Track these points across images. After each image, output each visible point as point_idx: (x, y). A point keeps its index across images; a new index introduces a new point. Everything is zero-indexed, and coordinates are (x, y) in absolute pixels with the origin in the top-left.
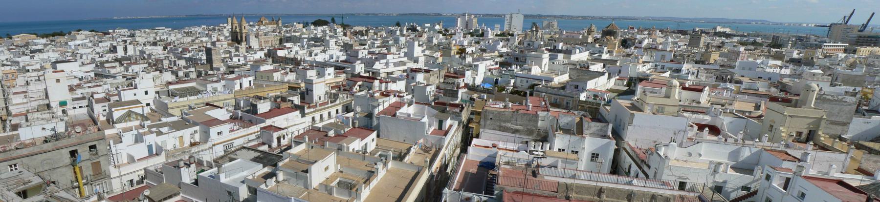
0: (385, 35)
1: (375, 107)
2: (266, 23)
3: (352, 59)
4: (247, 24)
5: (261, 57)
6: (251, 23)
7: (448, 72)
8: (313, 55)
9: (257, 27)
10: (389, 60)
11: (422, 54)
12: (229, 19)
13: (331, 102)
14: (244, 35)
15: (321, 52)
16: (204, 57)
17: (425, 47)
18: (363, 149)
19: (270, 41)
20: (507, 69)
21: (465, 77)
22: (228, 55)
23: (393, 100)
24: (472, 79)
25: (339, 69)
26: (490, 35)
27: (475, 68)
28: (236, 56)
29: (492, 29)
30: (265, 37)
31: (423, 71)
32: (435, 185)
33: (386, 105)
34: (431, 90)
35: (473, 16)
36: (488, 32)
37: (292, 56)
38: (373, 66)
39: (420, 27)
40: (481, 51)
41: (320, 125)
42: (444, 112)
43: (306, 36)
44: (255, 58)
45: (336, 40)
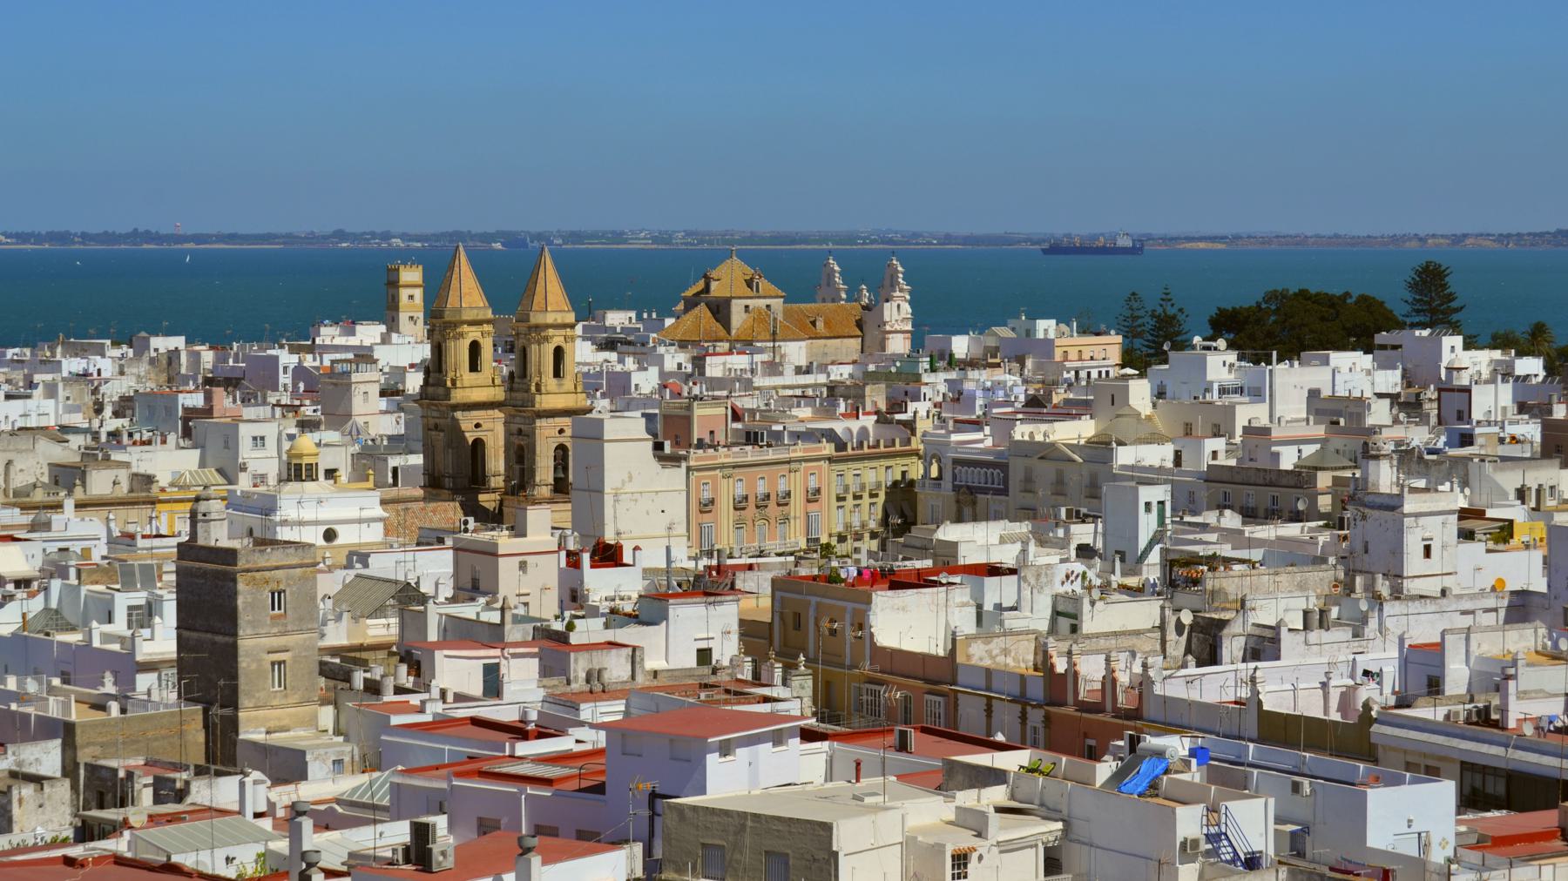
2: (763, 316)
5: (704, 656)
6: (617, 319)
8: (1232, 647)
9: (674, 359)
12: (411, 275)
14: (547, 436)
15: (1315, 620)
16: (162, 641)
22: (383, 629)
28: (463, 634)
30: (751, 454)
37: (1020, 658)
43: (1158, 455)
44: (653, 662)
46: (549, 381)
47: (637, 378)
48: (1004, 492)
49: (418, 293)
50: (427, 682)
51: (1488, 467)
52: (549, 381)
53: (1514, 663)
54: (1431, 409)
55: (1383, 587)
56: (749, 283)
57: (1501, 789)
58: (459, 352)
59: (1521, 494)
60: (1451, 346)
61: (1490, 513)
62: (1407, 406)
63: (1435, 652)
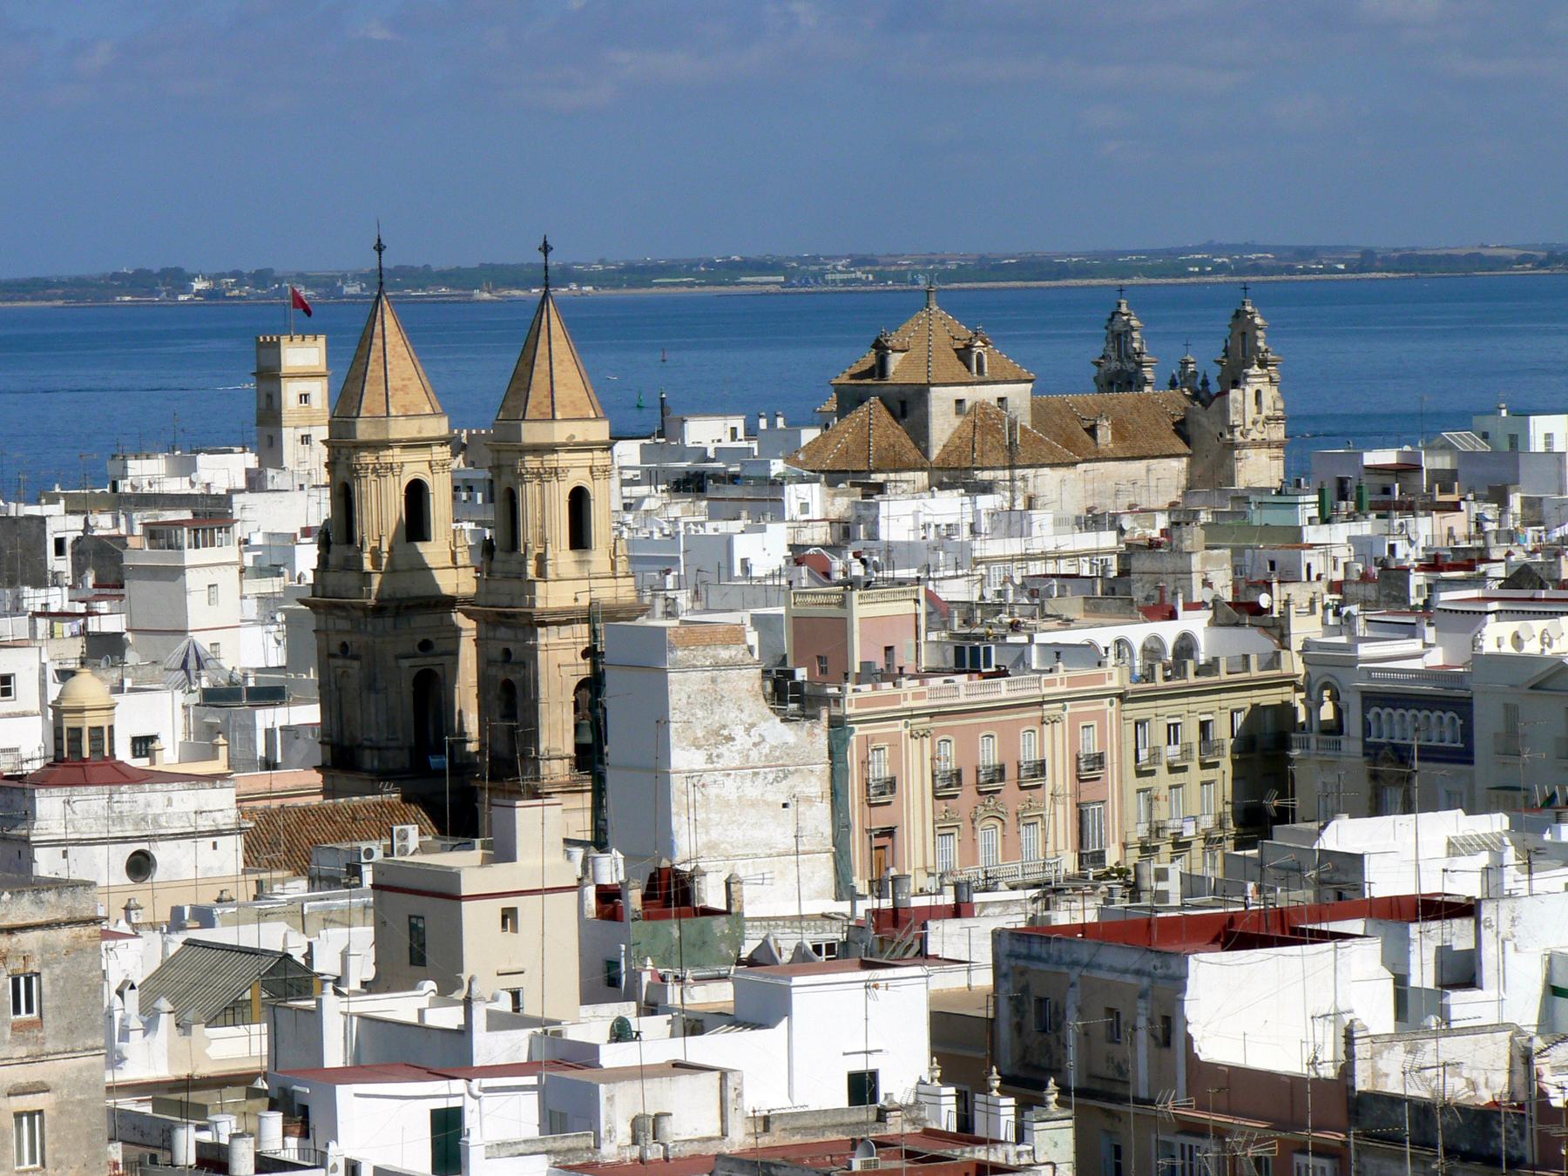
4: (629, 452)
5: (862, 1087)
19: (1059, 776)
46: (562, 557)
47: (744, 546)
48: (1464, 756)
49: (319, 391)
50: (320, 1147)
52: (562, 557)
56: (964, 354)
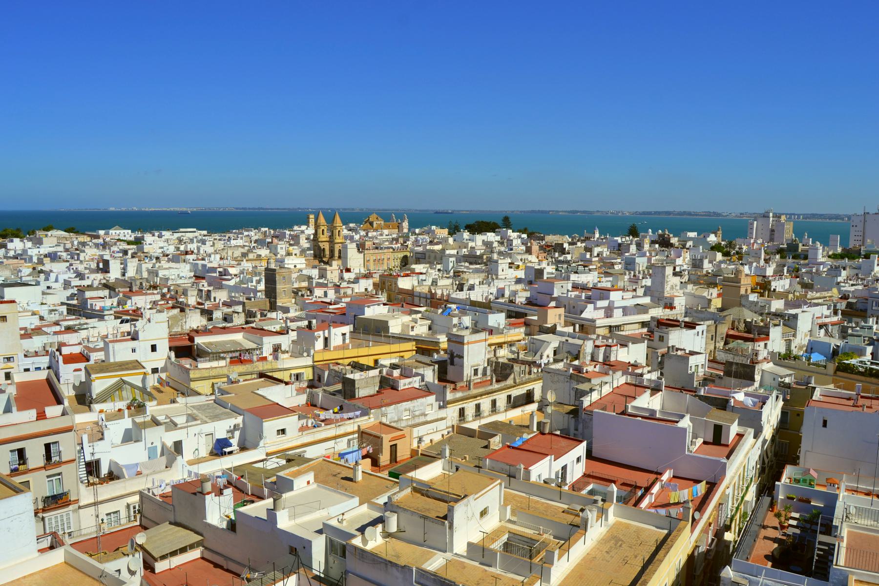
0: (606, 252)
1: (584, 393)
2: (379, 225)
3: (541, 299)
4: (344, 227)
5: (366, 289)
6: (352, 225)
7: (733, 329)
8: (465, 288)
9: (363, 233)
10: (613, 302)
11: (681, 291)
12: (312, 216)
13: (498, 381)
14: (337, 248)
15: (481, 283)
16: (262, 286)
17: (686, 278)
18: (557, 477)
19: (386, 260)
20: (857, 324)
21: (768, 339)
22: (305, 284)
23: (620, 379)
24: (783, 343)
25: (516, 317)
26: (820, 256)
27: (790, 322)
28: (320, 285)
29: (825, 243)
30: (376, 251)
31: (683, 324)
32: (705, 559)
33: (606, 389)
34: (698, 364)
35: (783, 218)
36: (817, 249)
37: (425, 290)
38: (582, 312)
39: (676, 239)
40: (802, 287)
41: (474, 425)
42: (725, 410)
43: (454, 252)
44: (356, 290)
45: (510, 261)
46: (337, 237)
47: (355, 236)
48: (425, 259)
49: (313, 220)
51: (515, 255)
52: (337, 237)
53: (517, 291)
54: (505, 244)
55: (494, 277)
56: (377, 218)
57: (514, 315)
58: (320, 231)
59: (521, 260)
60: (510, 231)
61: (515, 263)
62: (501, 243)
63: (503, 289)
